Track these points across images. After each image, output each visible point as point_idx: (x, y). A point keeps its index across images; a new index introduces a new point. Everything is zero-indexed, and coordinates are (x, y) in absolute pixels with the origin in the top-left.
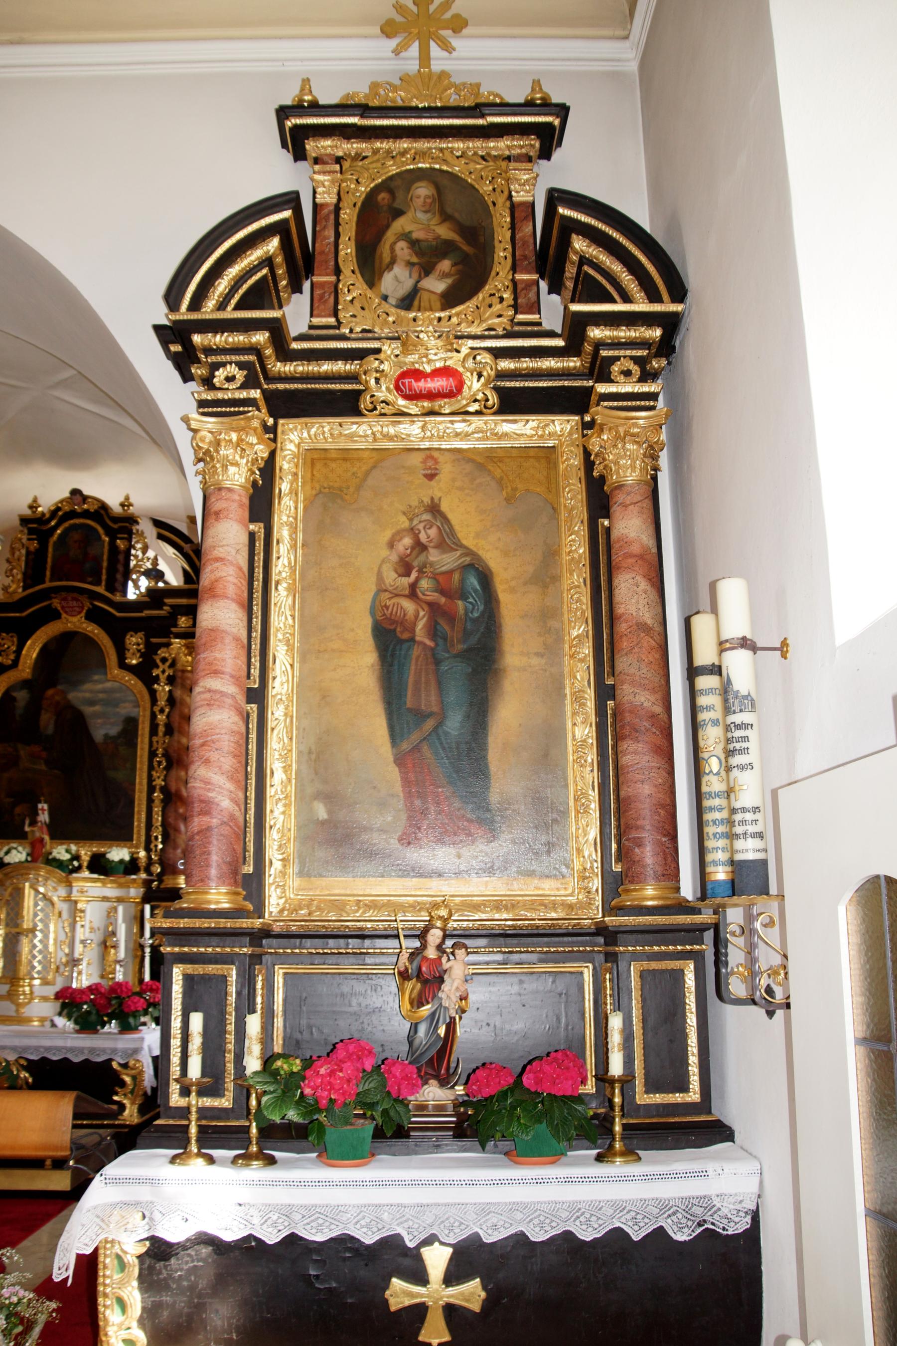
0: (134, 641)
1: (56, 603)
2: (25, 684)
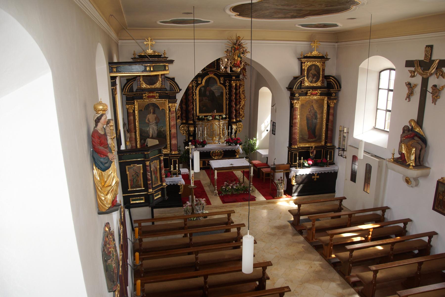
0: (222, 79)
2: (203, 86)
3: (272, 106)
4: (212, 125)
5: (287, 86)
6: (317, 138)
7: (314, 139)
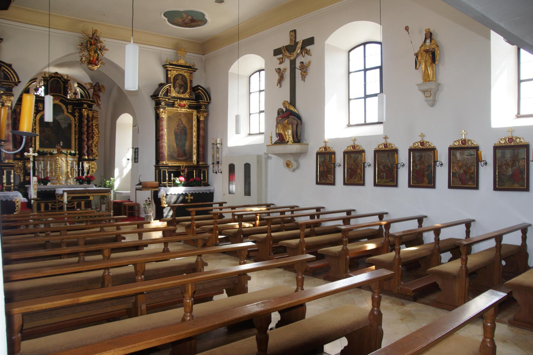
3: (134, 126)
4: (56, 161)
5: (152, 94)
6: (188, 156)
7: (184, 158)
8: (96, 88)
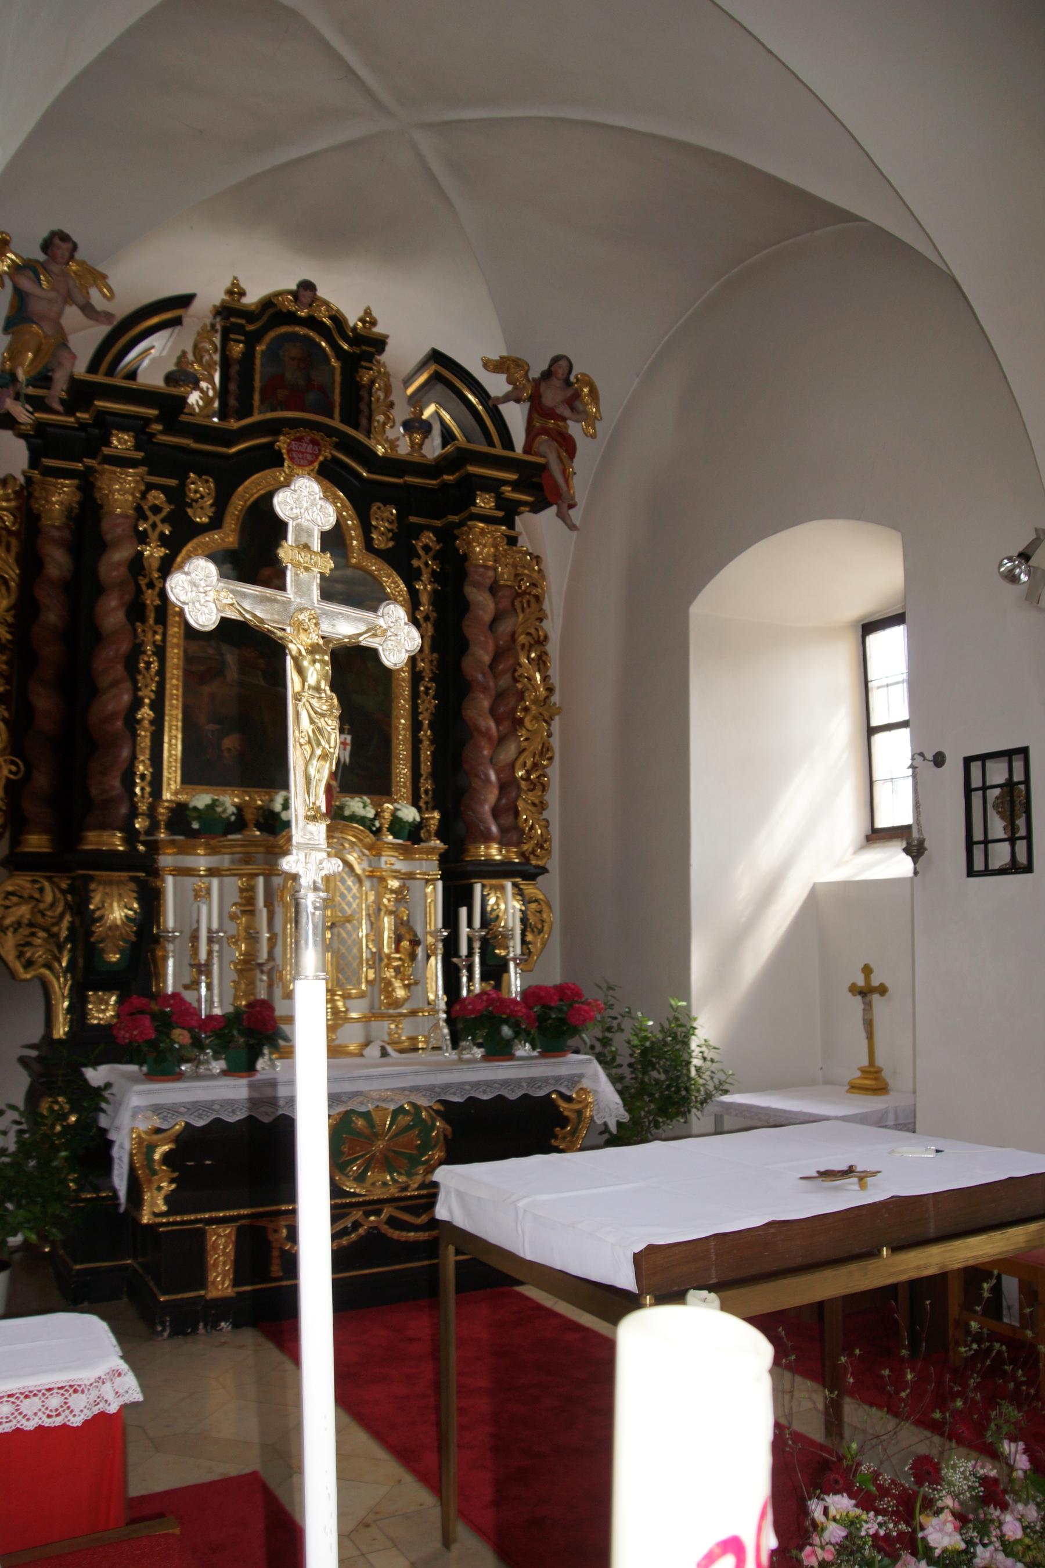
1: (282, 443)
8: (551, 397)
